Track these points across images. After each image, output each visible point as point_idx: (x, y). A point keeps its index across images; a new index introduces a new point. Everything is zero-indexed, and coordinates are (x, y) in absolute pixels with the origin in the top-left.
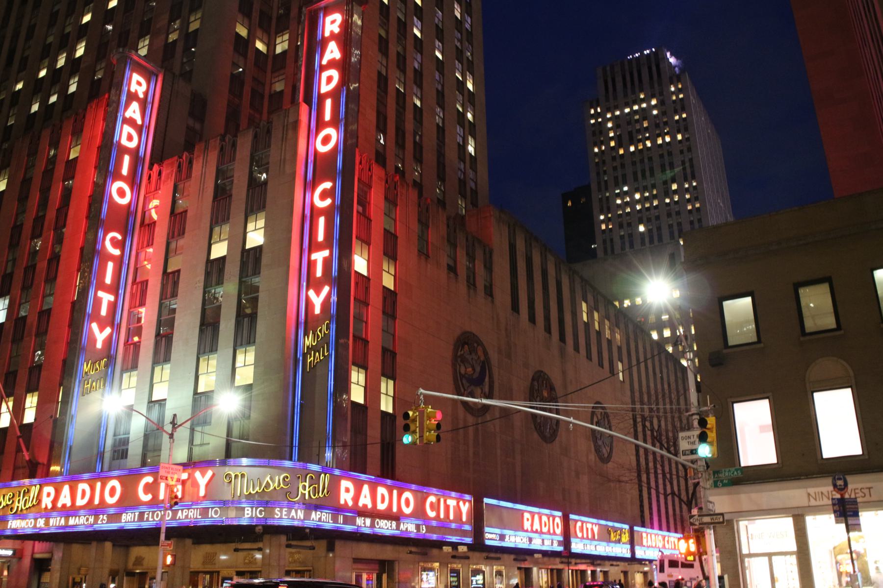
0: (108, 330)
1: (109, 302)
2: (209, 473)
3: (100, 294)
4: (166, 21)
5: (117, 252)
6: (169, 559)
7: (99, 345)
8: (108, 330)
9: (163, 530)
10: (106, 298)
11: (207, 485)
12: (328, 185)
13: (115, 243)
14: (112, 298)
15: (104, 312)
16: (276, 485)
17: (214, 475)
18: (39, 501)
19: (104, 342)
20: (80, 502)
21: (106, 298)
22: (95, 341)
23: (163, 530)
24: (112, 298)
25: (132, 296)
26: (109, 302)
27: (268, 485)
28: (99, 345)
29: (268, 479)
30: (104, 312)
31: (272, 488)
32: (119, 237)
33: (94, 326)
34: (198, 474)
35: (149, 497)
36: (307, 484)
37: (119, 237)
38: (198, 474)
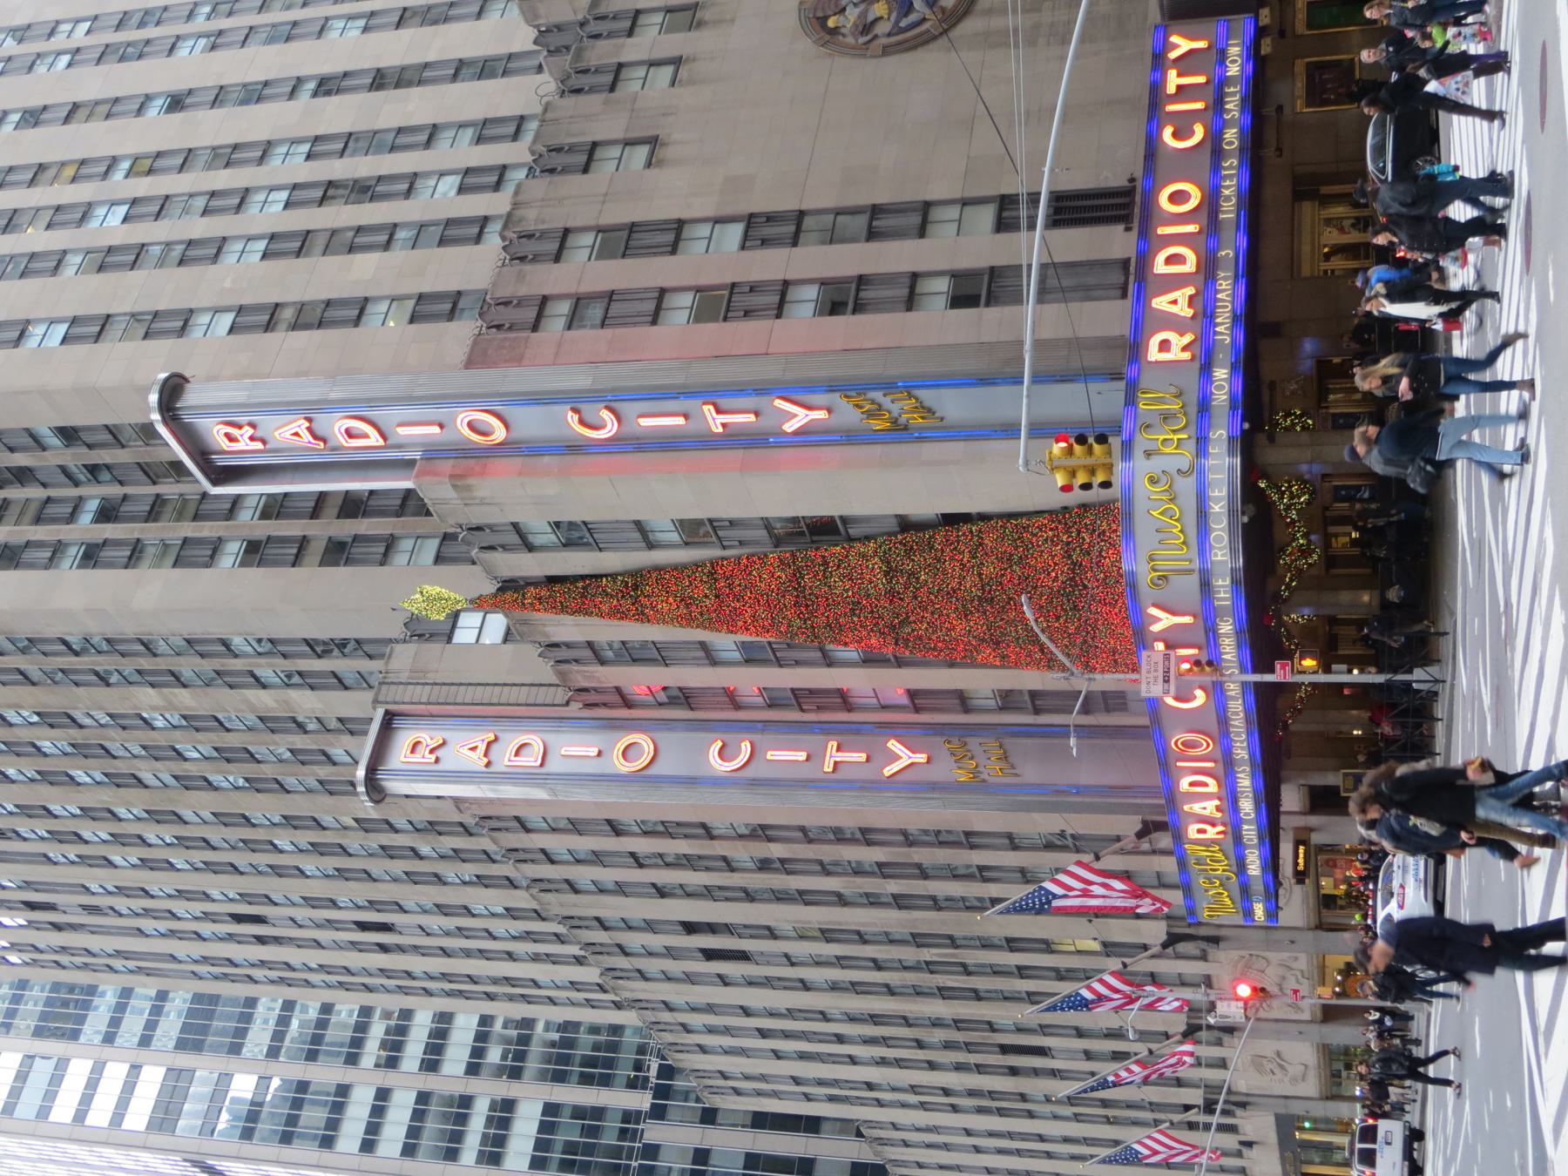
0: (893, 745)
2: (1153, 611)
4: (262, 692)
6: (1309, 663)
7: (921, 758)
9: (1258, 678)
11: (1174, 613)
12: (573, 419)
17: (1154, 605)
18: (1214, 841)
20: (1213, 786)
23: (1258, 678)
25: (819, 708)
34: (1156, 628)
35: (1199, 693)
38: (1156, 628)
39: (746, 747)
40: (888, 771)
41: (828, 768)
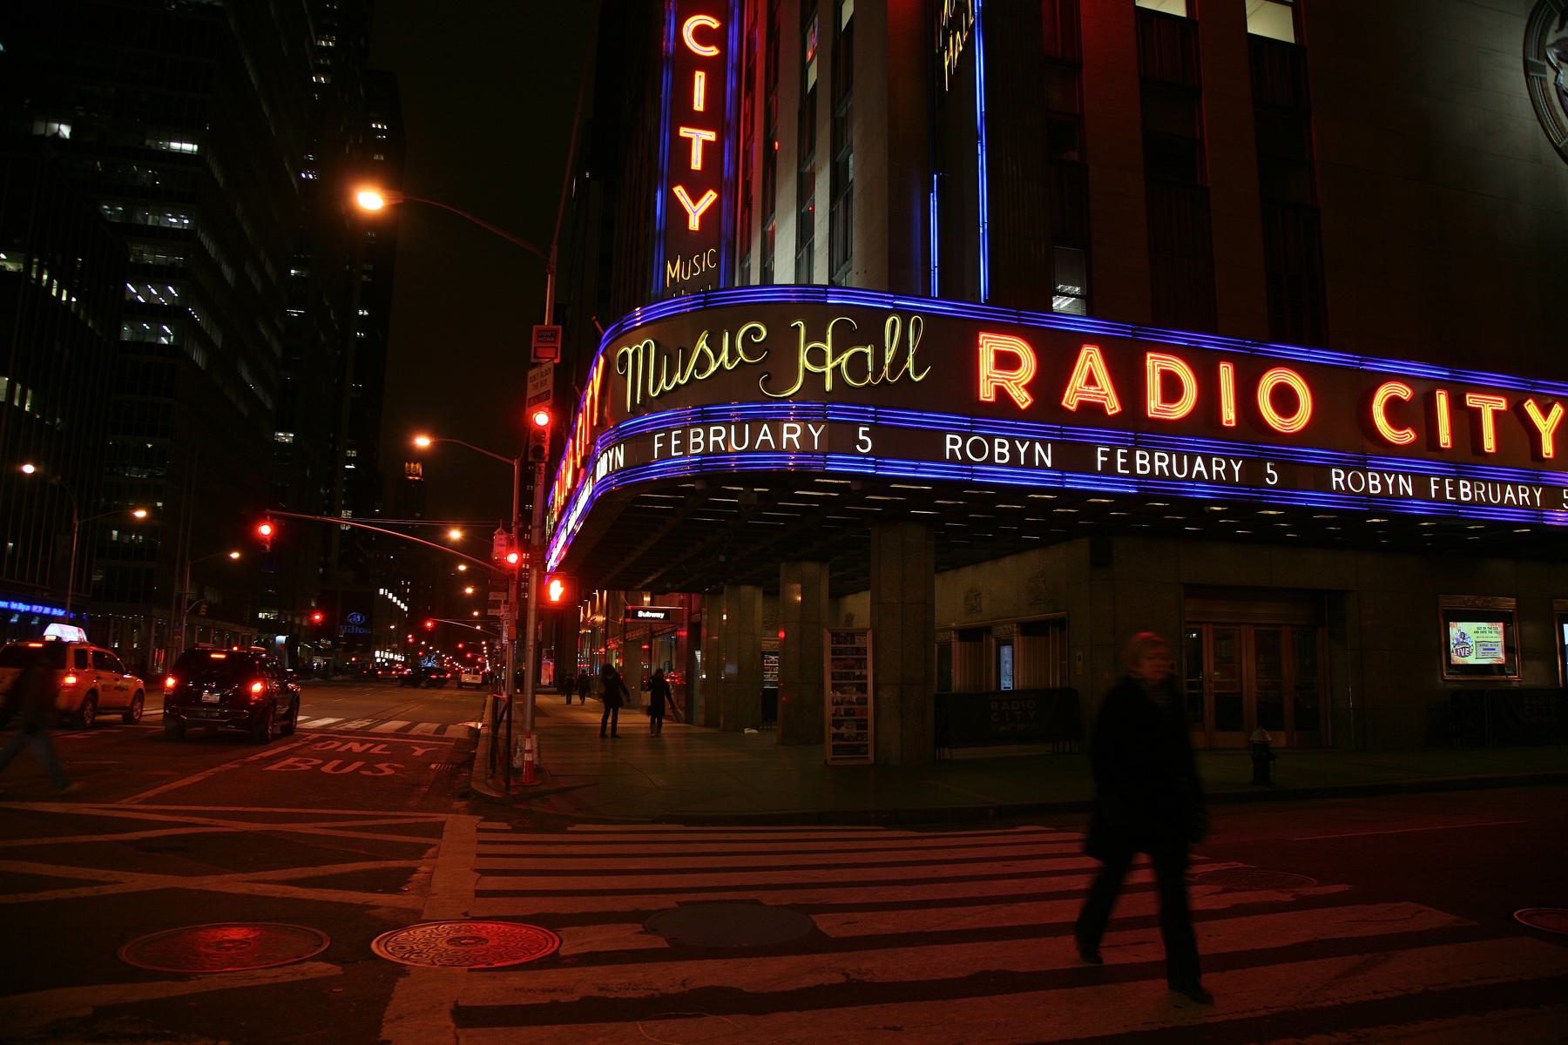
0: (710, 197)
1: (705, 143)
3: (684, 132)
5: (712, 51)
7: (694, 224)
8: (710, 197)
10: (699, 138)
13: (702, 34)
14: (711, 136)
15: (696, 163)
16: (725, 356)
19: (702, 218)
21: (699, 138)
22: (685, 216)
24: (711, 136)
26: (705, 143)
27: (702, 364)
28: (694, 224)
29: (702, 344)
30: (696, 163)
31: (713, 368)
32: (715, 24)
33: (679, 191)
36: (828, 348)
37: (715, 24)
39: (712, 51)
40: (679, 191)
41: (684, 132)
